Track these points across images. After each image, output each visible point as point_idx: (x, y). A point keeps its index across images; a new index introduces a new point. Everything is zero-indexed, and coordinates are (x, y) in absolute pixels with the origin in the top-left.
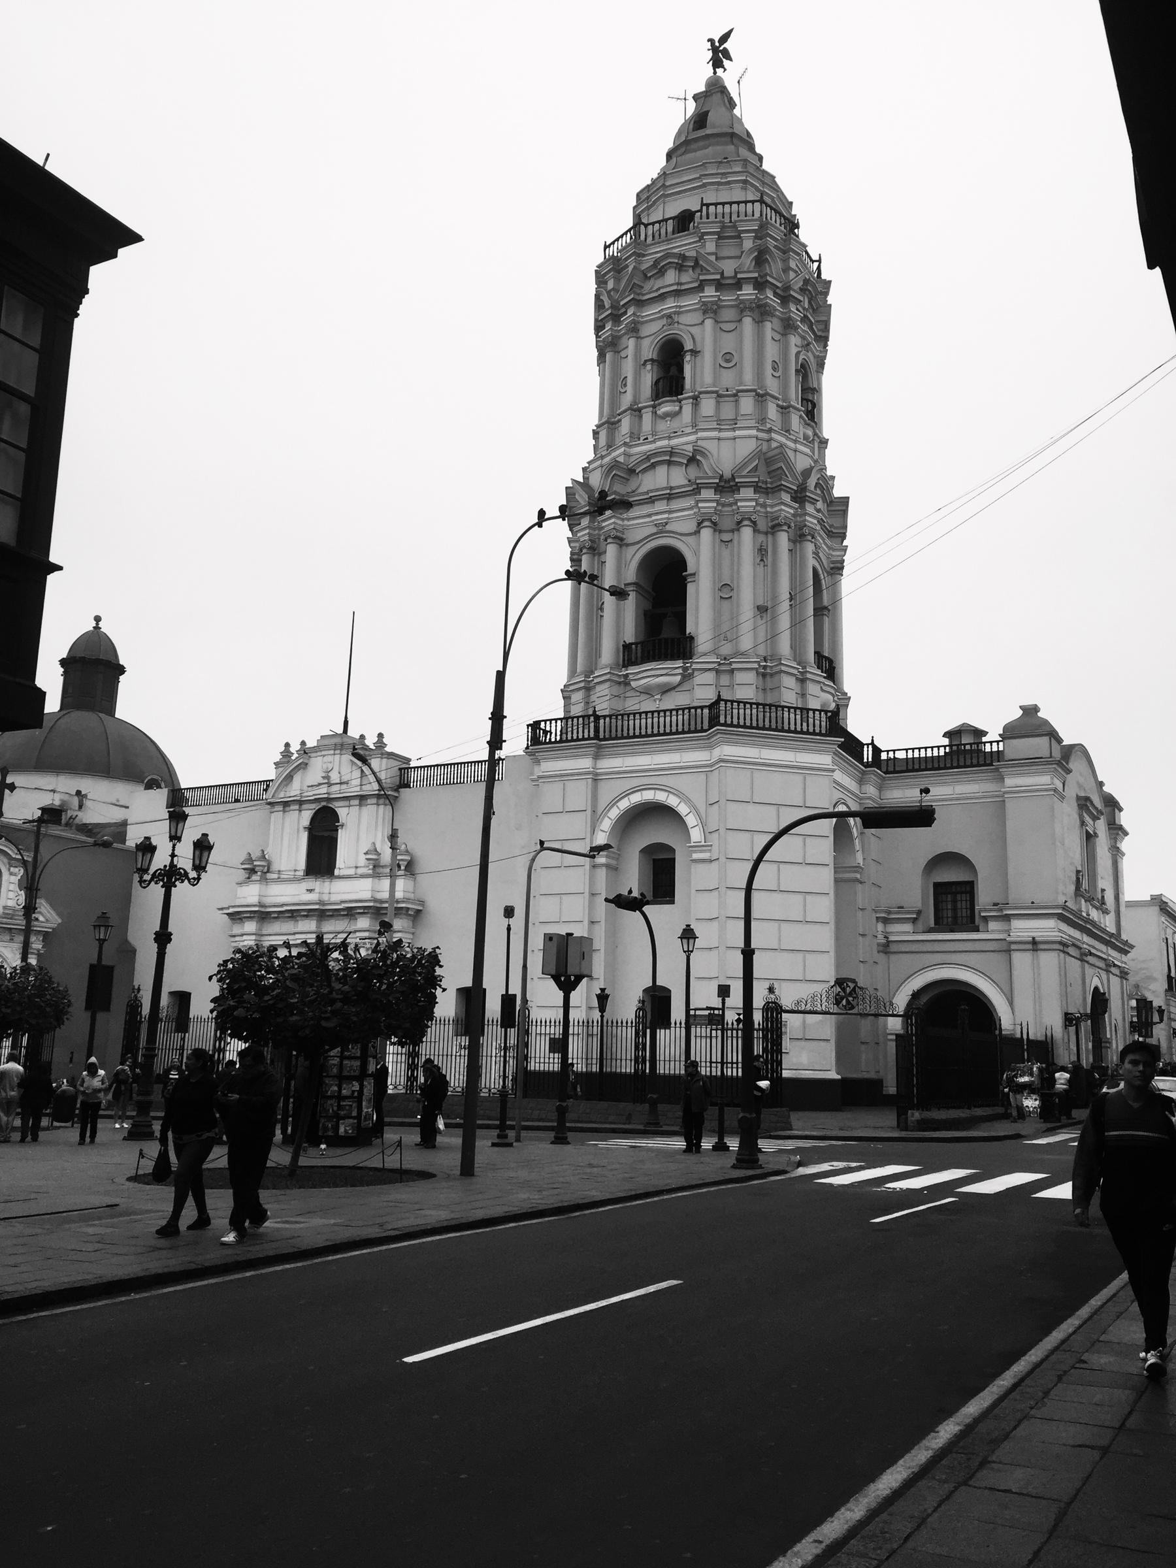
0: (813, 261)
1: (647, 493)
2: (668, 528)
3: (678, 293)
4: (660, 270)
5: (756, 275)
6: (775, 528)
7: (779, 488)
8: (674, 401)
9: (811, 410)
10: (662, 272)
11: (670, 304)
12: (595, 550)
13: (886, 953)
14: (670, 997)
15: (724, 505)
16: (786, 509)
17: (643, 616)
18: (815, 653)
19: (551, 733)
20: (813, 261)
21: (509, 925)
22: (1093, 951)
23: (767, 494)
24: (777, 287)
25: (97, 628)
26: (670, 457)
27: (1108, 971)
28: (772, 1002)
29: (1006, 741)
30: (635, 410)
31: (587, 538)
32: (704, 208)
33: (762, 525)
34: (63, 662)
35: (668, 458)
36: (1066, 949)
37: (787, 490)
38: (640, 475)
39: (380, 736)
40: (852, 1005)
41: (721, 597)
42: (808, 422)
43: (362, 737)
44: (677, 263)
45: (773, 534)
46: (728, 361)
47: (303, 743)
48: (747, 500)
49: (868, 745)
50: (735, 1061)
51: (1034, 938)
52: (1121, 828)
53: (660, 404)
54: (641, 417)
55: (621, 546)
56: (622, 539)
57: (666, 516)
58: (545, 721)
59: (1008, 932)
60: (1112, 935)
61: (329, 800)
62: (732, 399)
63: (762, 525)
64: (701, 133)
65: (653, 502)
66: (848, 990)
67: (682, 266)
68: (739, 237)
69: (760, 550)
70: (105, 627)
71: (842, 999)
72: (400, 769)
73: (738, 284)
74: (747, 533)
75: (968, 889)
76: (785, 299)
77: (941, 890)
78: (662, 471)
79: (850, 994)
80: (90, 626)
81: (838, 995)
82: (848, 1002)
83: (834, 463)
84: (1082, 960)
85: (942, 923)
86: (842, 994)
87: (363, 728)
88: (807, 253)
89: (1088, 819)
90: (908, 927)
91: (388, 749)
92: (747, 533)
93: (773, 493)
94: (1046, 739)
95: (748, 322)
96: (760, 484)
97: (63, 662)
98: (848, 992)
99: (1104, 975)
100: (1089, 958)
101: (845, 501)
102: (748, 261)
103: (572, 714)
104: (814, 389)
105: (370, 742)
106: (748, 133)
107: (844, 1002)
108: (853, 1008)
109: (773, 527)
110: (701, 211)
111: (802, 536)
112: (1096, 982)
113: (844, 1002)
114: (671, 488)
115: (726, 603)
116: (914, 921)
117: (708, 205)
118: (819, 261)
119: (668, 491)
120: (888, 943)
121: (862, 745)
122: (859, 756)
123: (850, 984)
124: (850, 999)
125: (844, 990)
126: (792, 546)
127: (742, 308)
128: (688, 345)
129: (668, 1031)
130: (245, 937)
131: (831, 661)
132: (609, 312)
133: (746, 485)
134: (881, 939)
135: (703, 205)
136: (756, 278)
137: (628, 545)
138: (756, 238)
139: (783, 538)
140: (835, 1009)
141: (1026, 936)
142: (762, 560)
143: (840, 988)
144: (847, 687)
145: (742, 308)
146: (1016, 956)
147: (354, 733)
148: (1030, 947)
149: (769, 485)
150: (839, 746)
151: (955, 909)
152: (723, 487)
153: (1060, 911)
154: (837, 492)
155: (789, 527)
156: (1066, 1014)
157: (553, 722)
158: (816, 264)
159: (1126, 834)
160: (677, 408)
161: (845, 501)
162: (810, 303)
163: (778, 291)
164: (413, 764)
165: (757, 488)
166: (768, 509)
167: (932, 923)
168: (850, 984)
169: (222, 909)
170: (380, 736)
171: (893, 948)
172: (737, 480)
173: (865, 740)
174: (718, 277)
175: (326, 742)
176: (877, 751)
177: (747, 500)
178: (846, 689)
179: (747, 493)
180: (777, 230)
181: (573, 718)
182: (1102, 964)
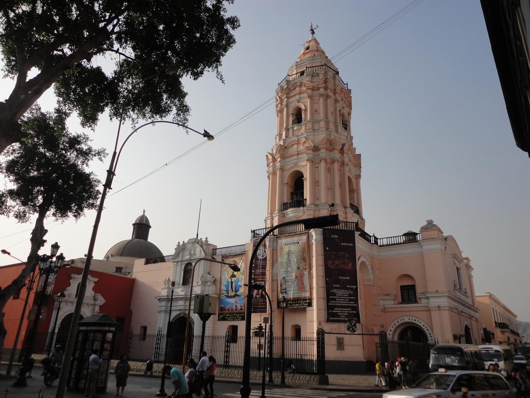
0: (345, 84)
1: (290, 154)
2: (298, 164)
3: (300, 93)
4: (294, 88)
5: (324, 86)
6: (333, 162)
7: (333, 149)
9: (346, 126)
10: (295, 88)
11: (298, 96)
12: (274, 173)
13: (384, 312)
14: (300, 329)
15: (315, 156)
16: (337, 155)
17: (290, 194)
18: (350, 204)
19: (260, 235)
20: (345, 84)
21: (173, 290)
22: (463, 311)
23: (330, 151)
24: (332, 89)
25: (144, 214)
27: (470, 319)
28: (320, 329)
29: (422, 233)
30: (287, 129)
31: (272, 170)
32: (307, 69)
33: (329, 161)
34: (134, 225)
36: (451, 309)
39: (207, 238)
42: (345, 130)
43: (201, 239)
45: (333, 164)
46: (316, 112)
47: (184, 242)
48: (323, 153)
49: (372, 236)
50: (306, 354)
51: (439, 306)
52: (470, 267)
53: (294, 127)
54: (289, 131)
55: (283, 171)
58: (257, 230)
59: (429, 303)
60: (471, 305)
61: (191, 260)
62: (318, 123)
63: (329, 161)
64: (308, 51)
65: (292, 156)
66: (353, 324)
67: (301, 86)
68: (318, 76)
69: (328, 170)
70: (146, 214)
71: (350, 327)
72: (213, 249)
73: (319, 89)
74: (323, 164)
75: (412, 288)
76: (335, 93)
77: (403, 288)
79: (354, 326)
80: (142, 214)
81: (348, 326)
82: (353, 329)
83: (356, 144)
84: (459, 314)
85: (404, 300)
86: (350, 325)
87: (202, 237)
88: (341, 80)
89: (457, 262)
90: (392, 302)
91: (209, 243)
92: (323, 164)
93: (332, 151)
94: (436, 231)
95: (321, 100)
96: (327, 148)
97: (134, 225)
98: (353, 325)
99: (469, 320)
100: (463, 314)
101: (360, 155)
102: (322, 82)
103: (267, 227)
104: (347, 121)
105: (204, 240)
106: (323, 51)
107: (351, 329)
108: (355, 331)
109: (333, 162)
110: (306, 70)
111: (344, 165)
112: (466, 323)
113: (351, 329)
114: (298, 152)
115: (317, 187)
116: (394, 300)
117: (308, 68)
118: (347, 84)
120: (385, 309)
121: (370, 236)
122: (369, 241)
123: (353, 321)
124: (354, 328)
125: (351, 324)
126: (340, 168)
127: (321, 95)
128: (303, 107)
129: (300, 342)
130: (162, 307)
131: (357, 207)
132: (279, 102)
134: (382, 307)
135: (307, 68)
136: (324, 87)
137: (284, 171)
138: (324, 75)
139: (336, 166)
140: (348, 332)
141: (436, 305)
144: (364, 217)
145: (321, 95)
146: (432, 313)
147: (199, 238)
148: (437, 309)
150: (359, 235)
151: (409, 295)
152: (315, 150)
153: (447, 295)
154: (357, 153)
155: (338, 162)
156: (454, 335)
157: (261, 230)
158: (346, 85)
159: (473, 269)
160: (300, 127)
161: (360, 155)
162: (344, 95)
163: (332, 91)
164: (217, 248)
165: (326, 149)
167: (400, 300)
168: (353, 321)
169: (156, 298)
170: (207, 238)
171: (387, 310)
172: (319, 147)
173: (371, 234)
174: (312, 87)
175: (190, 241)
176: (376, 239)
177: (323, 153)
178: (363, 217)
179: (323, 151)
180: (331, 74)
181: (267, 228)
182: (467, 316)
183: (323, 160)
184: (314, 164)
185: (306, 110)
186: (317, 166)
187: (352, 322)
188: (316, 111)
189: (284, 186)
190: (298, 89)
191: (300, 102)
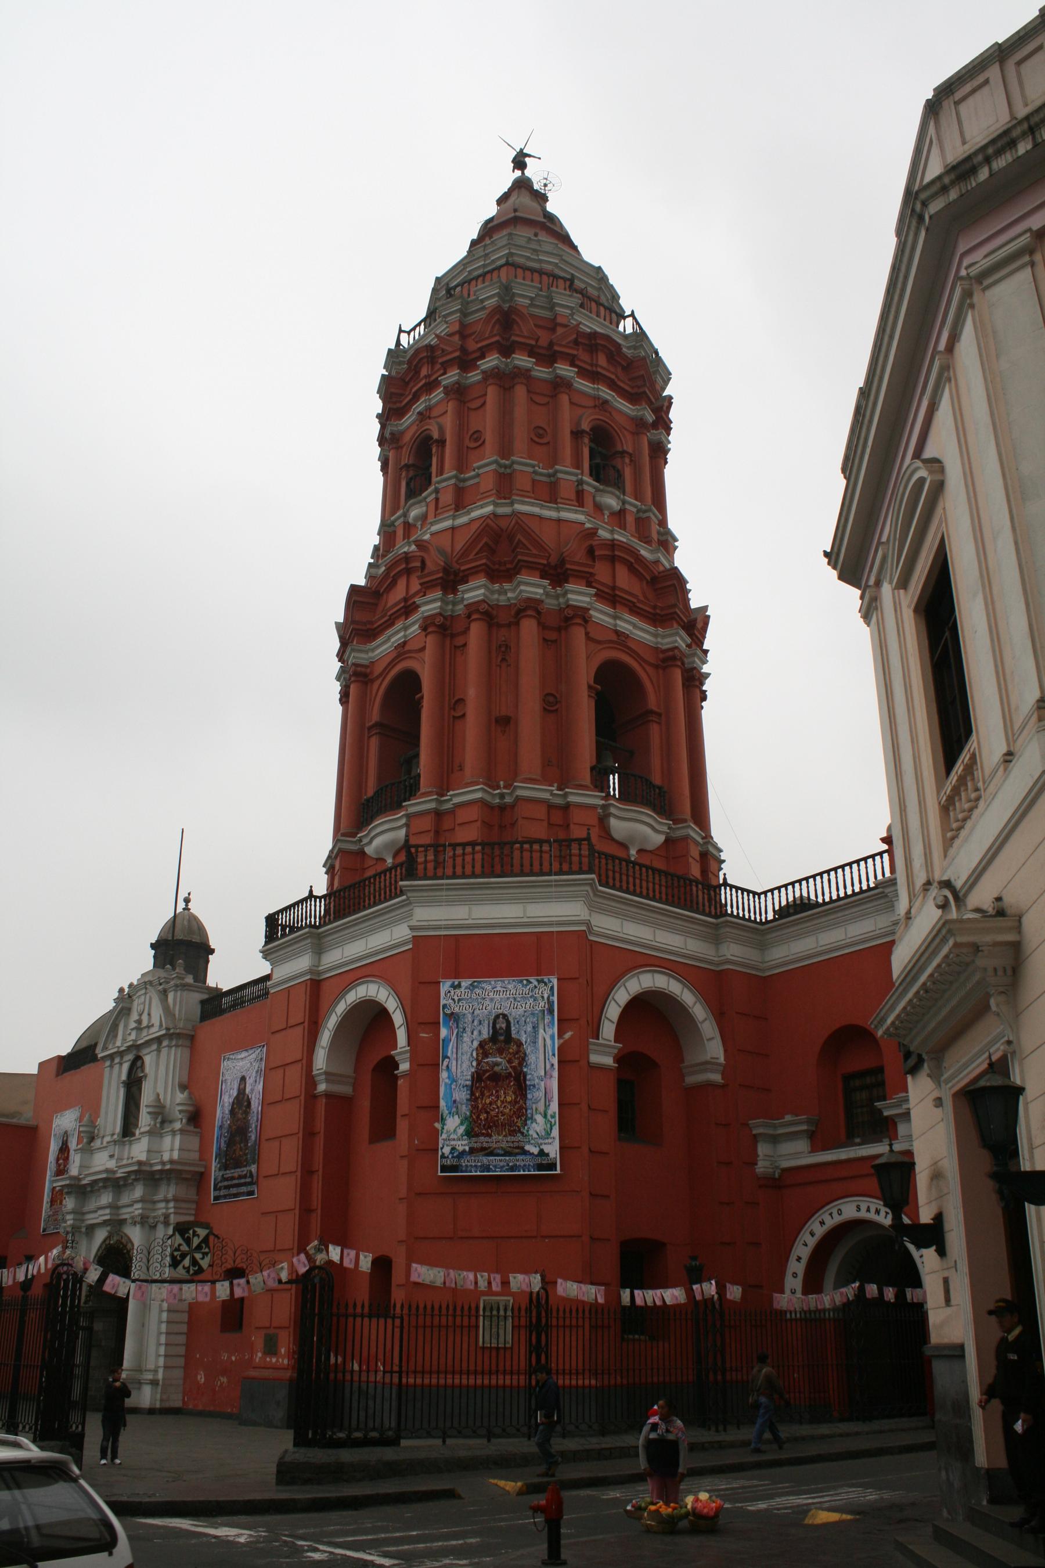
2: (407, 648)
8: (420, 502)
10: (417, 372)
26: (407, 563)
35: (404, 566)
37: (531, 567)
38: (385, 596)
40: (200, 1267)
41: (454, 717)
44: (427, 357)
46: (476, 440)
56: (365, 675)
57: (402, 634)
66: (196, 1241)
71: (183, 1256)
78: (402, 584)
86: (185, 1248)
98: (195, 1245)
113: (187, 1262)
119: (402, 605)
123: (199, 1231)
124: (198, 1256)
125: (188, 1241)
128: (436, 435)
133: (474, 572)
137: (372, 681)
142: (503, 660)
143: (184, 1239)
149: (509, 566)
166: (510, 595)
183: (474, 617)
184: (453, 636)
185: (442, 442)
186: (459, 641)
187: (195, 1234)
188: (477, 436)
189: (369, 737)
190: (424, 372)
191: (430, 418)
